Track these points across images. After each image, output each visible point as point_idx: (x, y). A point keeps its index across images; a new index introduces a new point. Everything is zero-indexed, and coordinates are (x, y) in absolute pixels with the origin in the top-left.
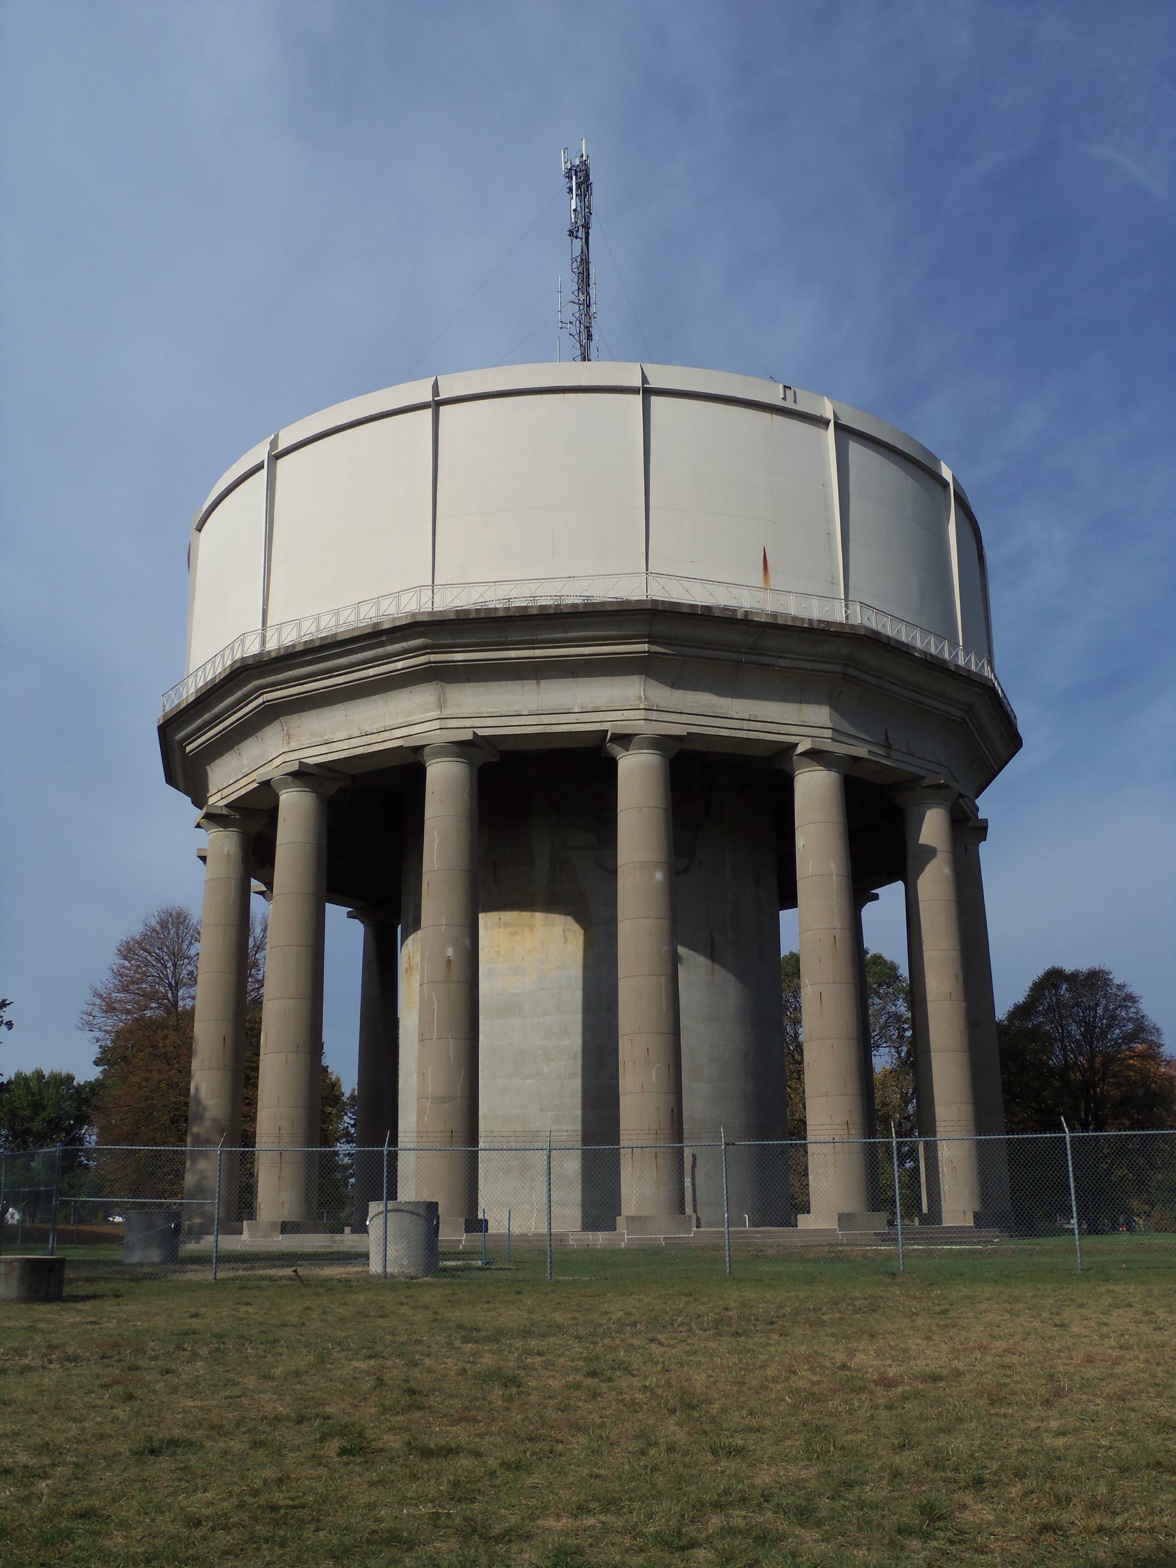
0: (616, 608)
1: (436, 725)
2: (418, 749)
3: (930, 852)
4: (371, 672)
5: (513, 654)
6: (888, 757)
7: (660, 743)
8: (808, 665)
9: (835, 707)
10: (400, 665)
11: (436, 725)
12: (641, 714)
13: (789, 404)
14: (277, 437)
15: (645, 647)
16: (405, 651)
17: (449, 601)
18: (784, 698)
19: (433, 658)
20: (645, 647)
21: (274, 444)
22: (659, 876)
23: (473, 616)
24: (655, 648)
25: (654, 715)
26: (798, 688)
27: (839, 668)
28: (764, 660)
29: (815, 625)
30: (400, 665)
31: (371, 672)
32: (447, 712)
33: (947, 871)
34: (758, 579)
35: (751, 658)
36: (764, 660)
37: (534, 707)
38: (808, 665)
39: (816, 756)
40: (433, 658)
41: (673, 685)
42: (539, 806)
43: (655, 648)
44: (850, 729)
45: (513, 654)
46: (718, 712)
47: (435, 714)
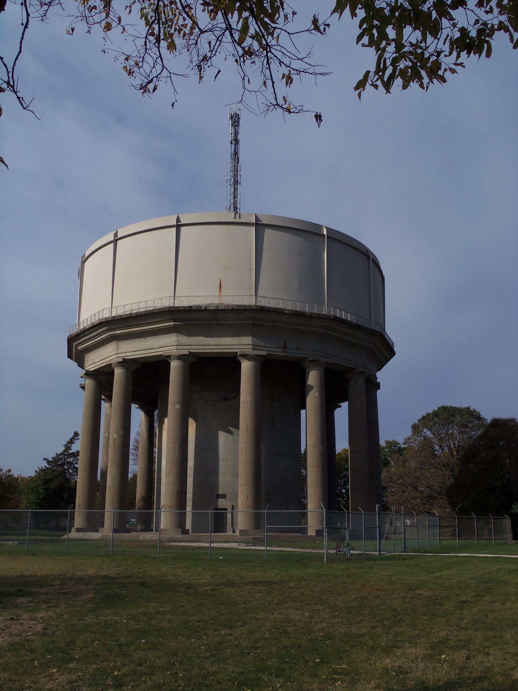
0: (158, 311)
1: (115, 356)
2: (169, 357)
3: (311, 387)
4: (98, 339)
5: (133, 329)
6: (285, 352)
7: (180, 357)
8: (238, 322)
9: (254, 335)
10: (104, 336)
11: (115, 356)
12: (175, 347)
13: (237, 220)
14: (117, 232)
15: (172, 323)
16: (103, 332)
17: (119, 311)
18: (233, 336)
19: (111, 333)
20: (172, 323)
21: (116, 235)
22: (178, 406)
23: (116, 318)
24: (176, 323)
25: (180, 347)
26: (237, 331)
27: (251, 322)
28: (219, 322)
29: (234, 308)
30: (104, 336)
31: (98, 339)
32: (120, 351)
33: (317, 394)
34: (217, 292)
35: (214, 322)
36: (219, 322)
37: (144, 347)
38: (238, 322)
39: (245, 356)
40: (111, 333)
41: (188, 335)
42: (212, 375)
43: (176, 323)
44: (263, 344)
45: (133, 329)
46: (205, 343)
47: (115, 352)
